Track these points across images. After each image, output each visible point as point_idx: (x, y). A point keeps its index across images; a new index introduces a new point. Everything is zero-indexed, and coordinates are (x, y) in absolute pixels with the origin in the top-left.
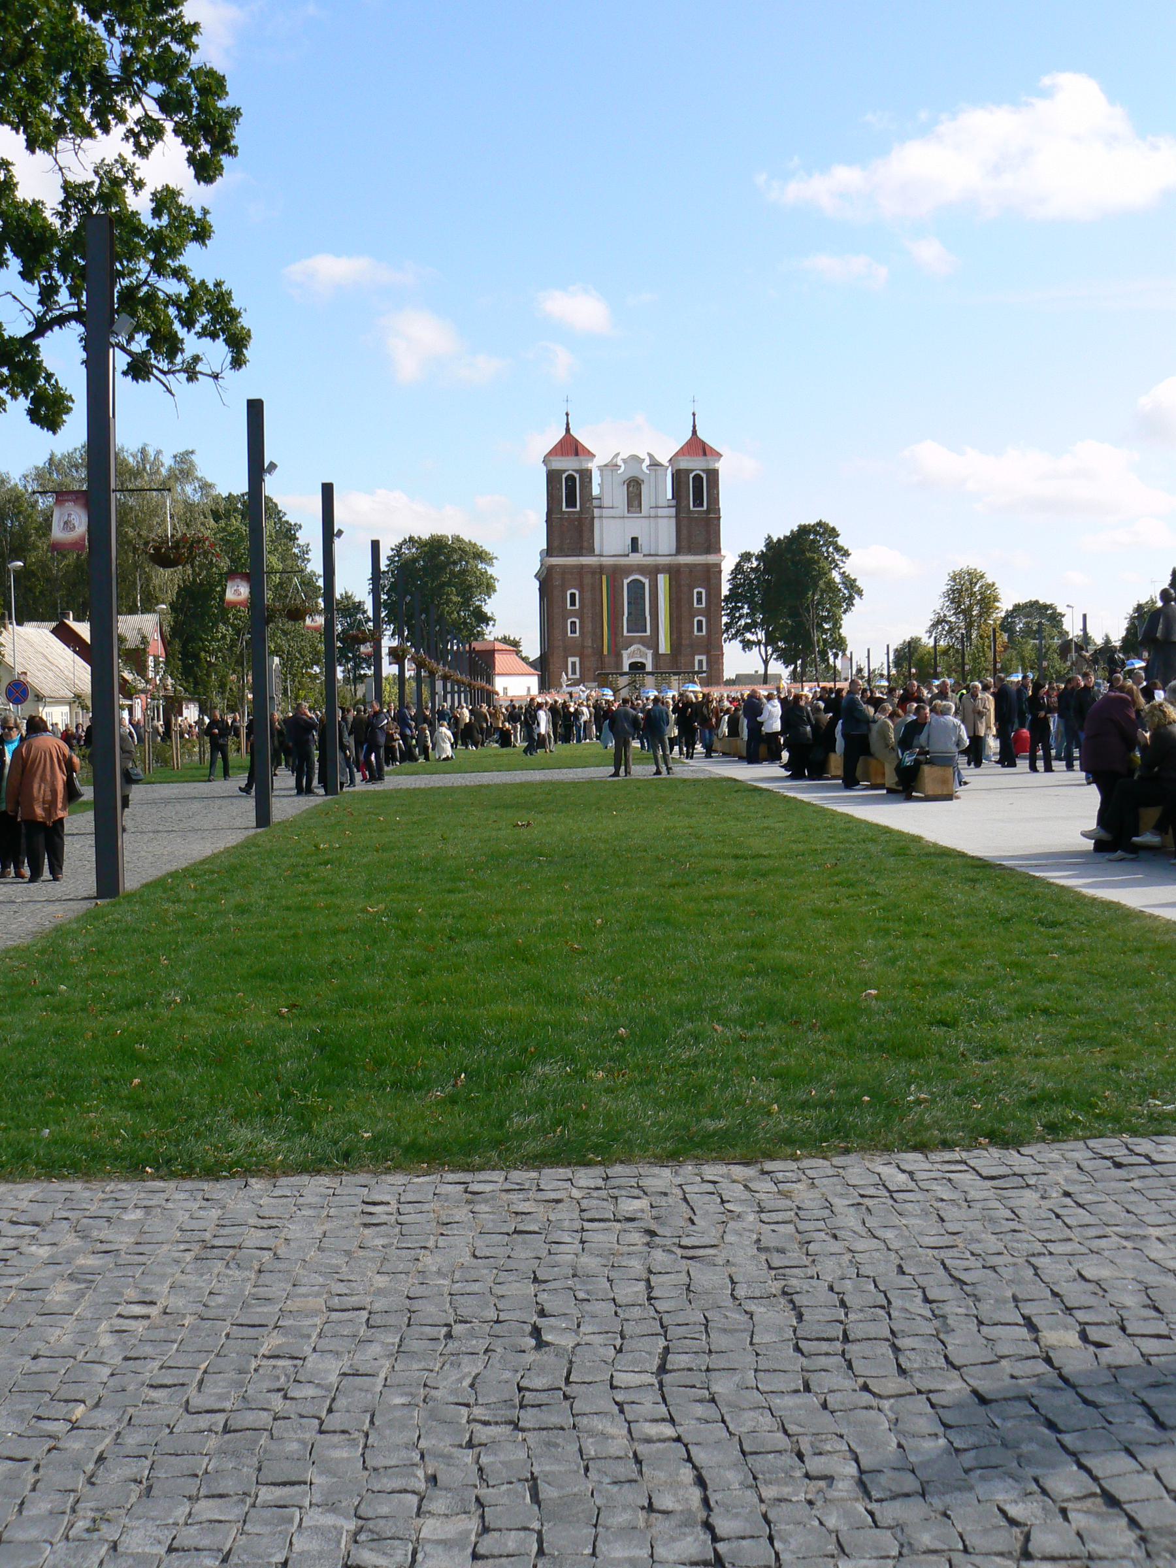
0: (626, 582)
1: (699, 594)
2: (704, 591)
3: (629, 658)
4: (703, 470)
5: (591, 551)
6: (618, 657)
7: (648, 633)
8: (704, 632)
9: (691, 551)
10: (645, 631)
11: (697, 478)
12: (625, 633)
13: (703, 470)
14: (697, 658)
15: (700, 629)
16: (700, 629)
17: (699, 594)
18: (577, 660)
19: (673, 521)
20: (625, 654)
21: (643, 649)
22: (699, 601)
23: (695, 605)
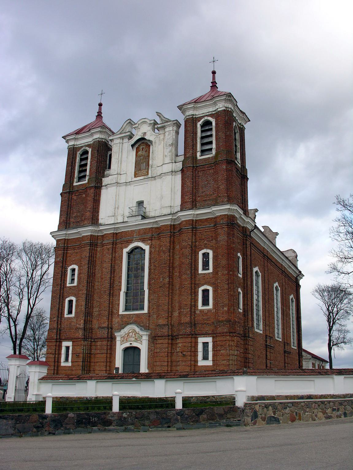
0: (126, 251)
1: (206, 255)
2: (211, 252)
3: (122, 342)
4: (211, 115)
5: (94, 220)
6: (112, 339)
7: (146, 311)
8: (211, 306)
9: (194, 206)
10: (142, 308)
11: (208, 123)
12: (121, 312)
13: (211, 115)
14: (201, 340)
15: (205, 302)
16: (205, 302)
17: (206, 255)
18: (69, 344)
19: (179, 177)
20: (118, 336)
21: (137, 329)
22: (206, 265)
23: (200, 271)
